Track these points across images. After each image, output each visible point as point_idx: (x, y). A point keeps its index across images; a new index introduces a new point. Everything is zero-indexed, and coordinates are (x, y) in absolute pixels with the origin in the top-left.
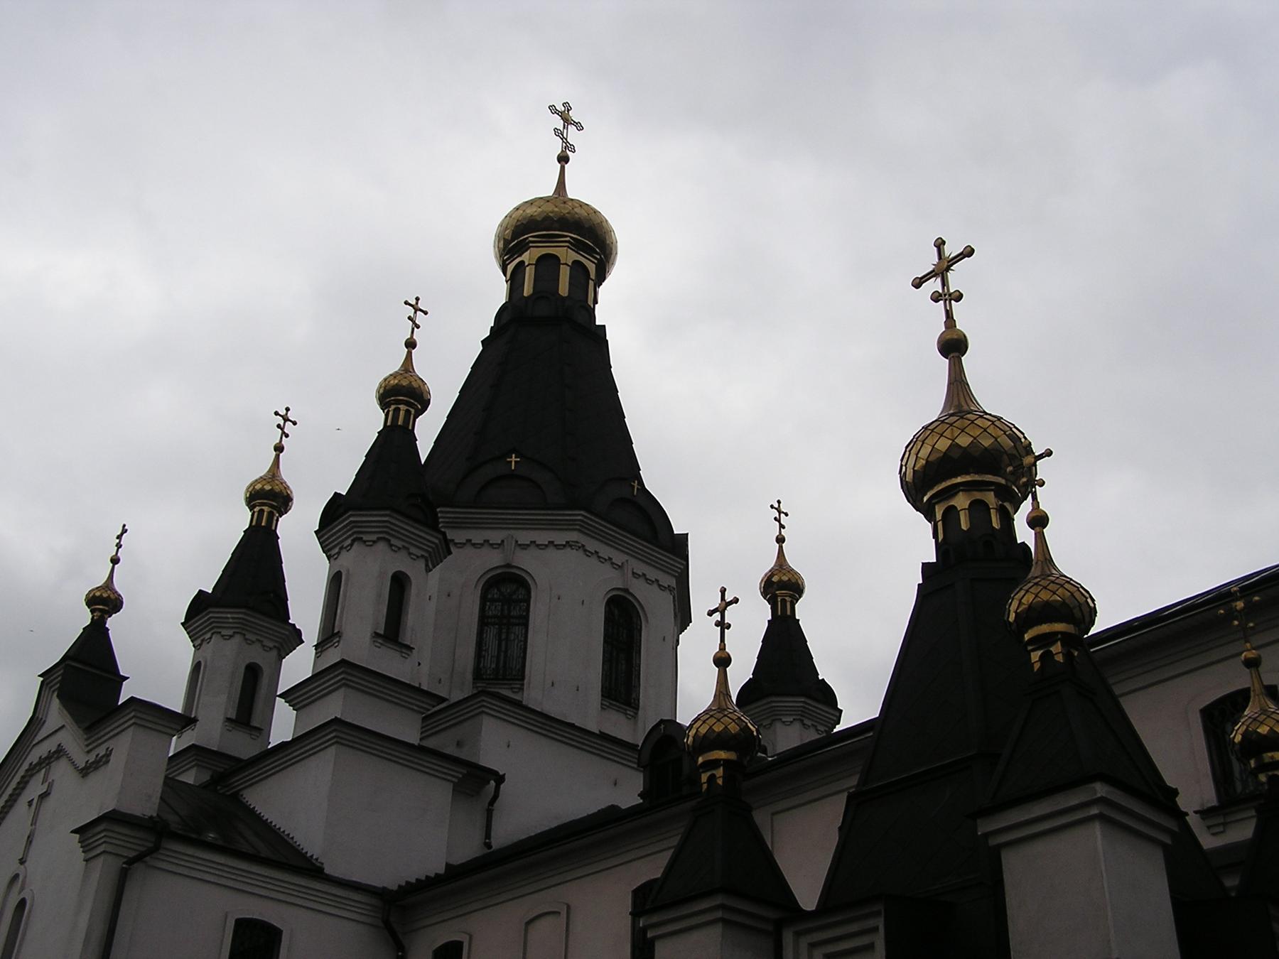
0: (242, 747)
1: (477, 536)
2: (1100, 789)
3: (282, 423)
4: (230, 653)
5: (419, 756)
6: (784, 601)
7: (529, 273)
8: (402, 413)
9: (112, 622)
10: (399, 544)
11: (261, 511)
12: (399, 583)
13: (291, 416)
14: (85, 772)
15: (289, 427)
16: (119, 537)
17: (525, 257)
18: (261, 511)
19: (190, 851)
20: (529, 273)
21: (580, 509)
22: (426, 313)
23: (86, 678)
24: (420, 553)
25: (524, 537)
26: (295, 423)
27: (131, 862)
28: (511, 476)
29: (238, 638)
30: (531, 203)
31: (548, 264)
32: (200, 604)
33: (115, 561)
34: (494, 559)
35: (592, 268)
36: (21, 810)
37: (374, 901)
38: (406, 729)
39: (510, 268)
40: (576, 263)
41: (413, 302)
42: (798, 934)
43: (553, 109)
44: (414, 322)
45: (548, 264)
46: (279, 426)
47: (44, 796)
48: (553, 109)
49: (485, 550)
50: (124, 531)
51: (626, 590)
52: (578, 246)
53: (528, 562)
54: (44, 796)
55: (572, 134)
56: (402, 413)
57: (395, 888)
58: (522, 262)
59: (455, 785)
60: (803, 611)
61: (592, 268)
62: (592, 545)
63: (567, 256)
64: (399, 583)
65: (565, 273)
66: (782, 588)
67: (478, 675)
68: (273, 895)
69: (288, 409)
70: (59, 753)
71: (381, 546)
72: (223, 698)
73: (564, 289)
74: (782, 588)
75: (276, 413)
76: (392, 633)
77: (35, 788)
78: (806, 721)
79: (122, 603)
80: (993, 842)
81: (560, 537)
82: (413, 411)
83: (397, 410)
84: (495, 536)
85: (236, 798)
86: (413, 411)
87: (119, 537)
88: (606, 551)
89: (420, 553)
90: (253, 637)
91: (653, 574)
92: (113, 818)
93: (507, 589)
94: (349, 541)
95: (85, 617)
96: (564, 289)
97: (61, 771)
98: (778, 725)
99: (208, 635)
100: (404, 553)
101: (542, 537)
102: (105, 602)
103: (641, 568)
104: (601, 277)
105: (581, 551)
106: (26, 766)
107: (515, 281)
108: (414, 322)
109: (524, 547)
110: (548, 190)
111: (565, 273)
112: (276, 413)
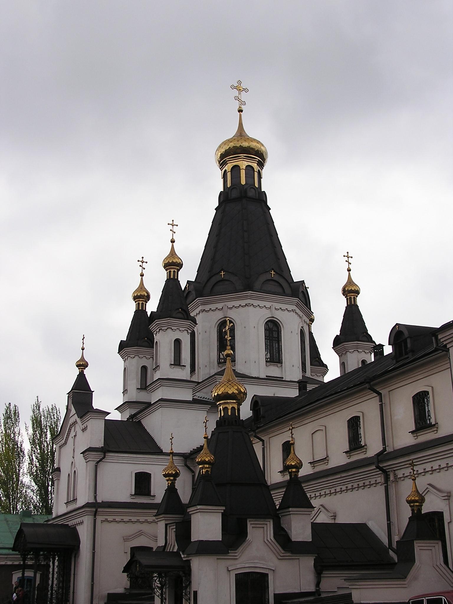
0: (143, 397)
1: (213, 306)
2: (199, 507)
3: (140, 263)
4: (136, 363)
5: (195, 401)
6: (350, 298)
7: (229, 175)
8: (172, 273)
9: (86, 372)
10: (175, 328)
11: (139, 304)
12: (178, 342)
13: (144, 260)
14: (84, 430)
15: (144, 265)
16: (83, 339)
17: (226, 168)
18: (139, 304)
19: (116, 455)
20: (229, 175)
22: (177, 226)
23: (81, 395)
24: (184, 329)
25: (230, 304)
26: (146, 263)
27: (98, 462)
28: (223, 280)
29: (137, 357)
30: (224, 143)
31: (236, 169)
32: (122, 346)
33: (83, 349)
34: (218, 316)
35: (255, 165)
36: (70, 440)
37: (182, 458)
38: (187, 395)
39: (224, 170)
41: (171, 223)
42: (170, 527)
43: (233, 87)
44: (173, 231)
45: (236, 169)
46: (140, 266)
47: (75, 436)
48: (233, 87)
49: (217, 311)
50: (84, 338)
51: (273, 317)
53: (233, 314)
54: (75, 436)
55: (244, 96)
56: (172, 273)
57: (189, 452)
58: (226, 170)
59: (207, 412)
60: (360, 301)
61: (255, 165)
62: (256, 303)
63: (243, 164)
64: (178, 342)
66: (351, 292)
67: (219, 363)
68: (147, 463)
69: (143, 258)
70: (75, 422)
71: (169, 330)
72: (135, 381)
73: (243, 182)
74: (351, 292)
75: (138, 261)
76: (177, 362)
77: (72, 434)
78: (359, 350)
79: (87, 363)
80: (190, 513)
81: (243, 303)
82: (176, 271)
83: (170, 272)
84: (220, 306)
85: (140, 422)
86: (176, 271)
87: (83, 339)
88: (262, 303)
89: (184, 329)
90: (142, 356)
91: (284, 307)
92: (90, 450)
94: (158, 330)
95: (77, 371)
96: (243, 182)
97: (79, 427)
98: (348, 353)
99: (126, 358)
100: (178, 330)
101: (236, 303)
102: (82, 365)
103: (278, 306)
104: (261, 164)
106: (69, 425)
107: (225, 176)
108: (173, 231)
109: (231, 308)
110: (232, 132)
112: (138, 261)
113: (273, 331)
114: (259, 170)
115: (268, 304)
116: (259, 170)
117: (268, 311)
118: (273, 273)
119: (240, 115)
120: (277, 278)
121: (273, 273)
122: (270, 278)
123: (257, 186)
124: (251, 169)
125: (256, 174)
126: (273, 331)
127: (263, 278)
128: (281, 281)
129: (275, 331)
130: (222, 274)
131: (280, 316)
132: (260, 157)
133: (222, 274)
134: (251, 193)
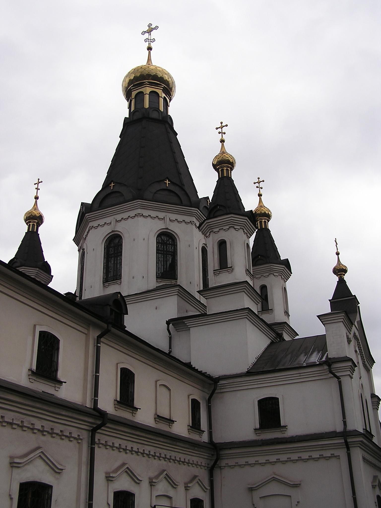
21: (138, 199)
25: (119, 217)
40: (150, 92)
49: (106, 226)
51: (167, 229)
52: (151, 84)
53: (120, 228)
61: (160, 92)
62: (146, 213)
63: (148, 90)
65: (147, 98)
73: (147, 105)
81: (132, 214)
84: (108, 220)
88: (153, 214)
93: (117, 241)
96: (147, 105)
101: (125, 215)
103: (174, 217)
105: (142, 217)
111: (147, 98)
113: (167, 244)
114: (164, 97)
115: (161, 215)
116: (164, 97)
117: (162, 222)
118: (167, 182)
119: (150, 53)
120: (173, 188)
121: (167, 182)
122: (166, 188)
123: (162, 111)
124: (154, 94)
125: (161, 101)
126: (167, 244)
127: (157, 187)
128: (176, 189)
129: (169, 244)
130: (112, 185)
131: (175, 228)
132: (168, 90)
133: (112, 185)
134: (154, 115)
